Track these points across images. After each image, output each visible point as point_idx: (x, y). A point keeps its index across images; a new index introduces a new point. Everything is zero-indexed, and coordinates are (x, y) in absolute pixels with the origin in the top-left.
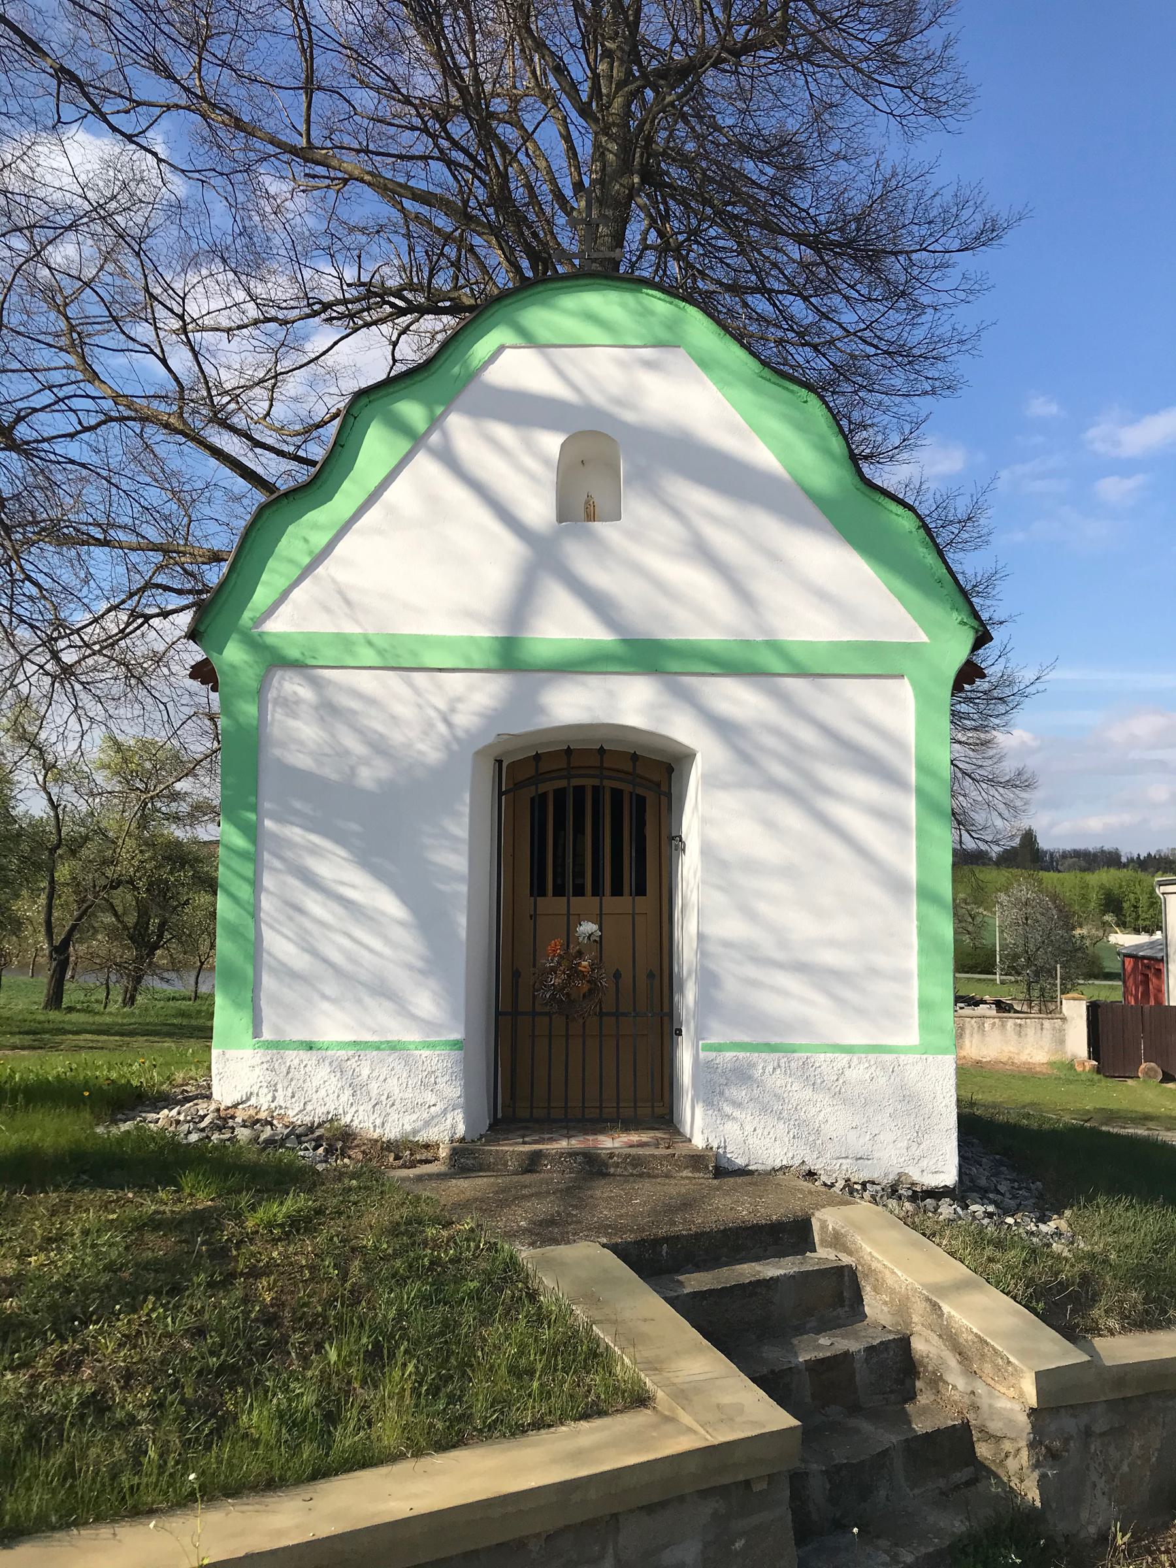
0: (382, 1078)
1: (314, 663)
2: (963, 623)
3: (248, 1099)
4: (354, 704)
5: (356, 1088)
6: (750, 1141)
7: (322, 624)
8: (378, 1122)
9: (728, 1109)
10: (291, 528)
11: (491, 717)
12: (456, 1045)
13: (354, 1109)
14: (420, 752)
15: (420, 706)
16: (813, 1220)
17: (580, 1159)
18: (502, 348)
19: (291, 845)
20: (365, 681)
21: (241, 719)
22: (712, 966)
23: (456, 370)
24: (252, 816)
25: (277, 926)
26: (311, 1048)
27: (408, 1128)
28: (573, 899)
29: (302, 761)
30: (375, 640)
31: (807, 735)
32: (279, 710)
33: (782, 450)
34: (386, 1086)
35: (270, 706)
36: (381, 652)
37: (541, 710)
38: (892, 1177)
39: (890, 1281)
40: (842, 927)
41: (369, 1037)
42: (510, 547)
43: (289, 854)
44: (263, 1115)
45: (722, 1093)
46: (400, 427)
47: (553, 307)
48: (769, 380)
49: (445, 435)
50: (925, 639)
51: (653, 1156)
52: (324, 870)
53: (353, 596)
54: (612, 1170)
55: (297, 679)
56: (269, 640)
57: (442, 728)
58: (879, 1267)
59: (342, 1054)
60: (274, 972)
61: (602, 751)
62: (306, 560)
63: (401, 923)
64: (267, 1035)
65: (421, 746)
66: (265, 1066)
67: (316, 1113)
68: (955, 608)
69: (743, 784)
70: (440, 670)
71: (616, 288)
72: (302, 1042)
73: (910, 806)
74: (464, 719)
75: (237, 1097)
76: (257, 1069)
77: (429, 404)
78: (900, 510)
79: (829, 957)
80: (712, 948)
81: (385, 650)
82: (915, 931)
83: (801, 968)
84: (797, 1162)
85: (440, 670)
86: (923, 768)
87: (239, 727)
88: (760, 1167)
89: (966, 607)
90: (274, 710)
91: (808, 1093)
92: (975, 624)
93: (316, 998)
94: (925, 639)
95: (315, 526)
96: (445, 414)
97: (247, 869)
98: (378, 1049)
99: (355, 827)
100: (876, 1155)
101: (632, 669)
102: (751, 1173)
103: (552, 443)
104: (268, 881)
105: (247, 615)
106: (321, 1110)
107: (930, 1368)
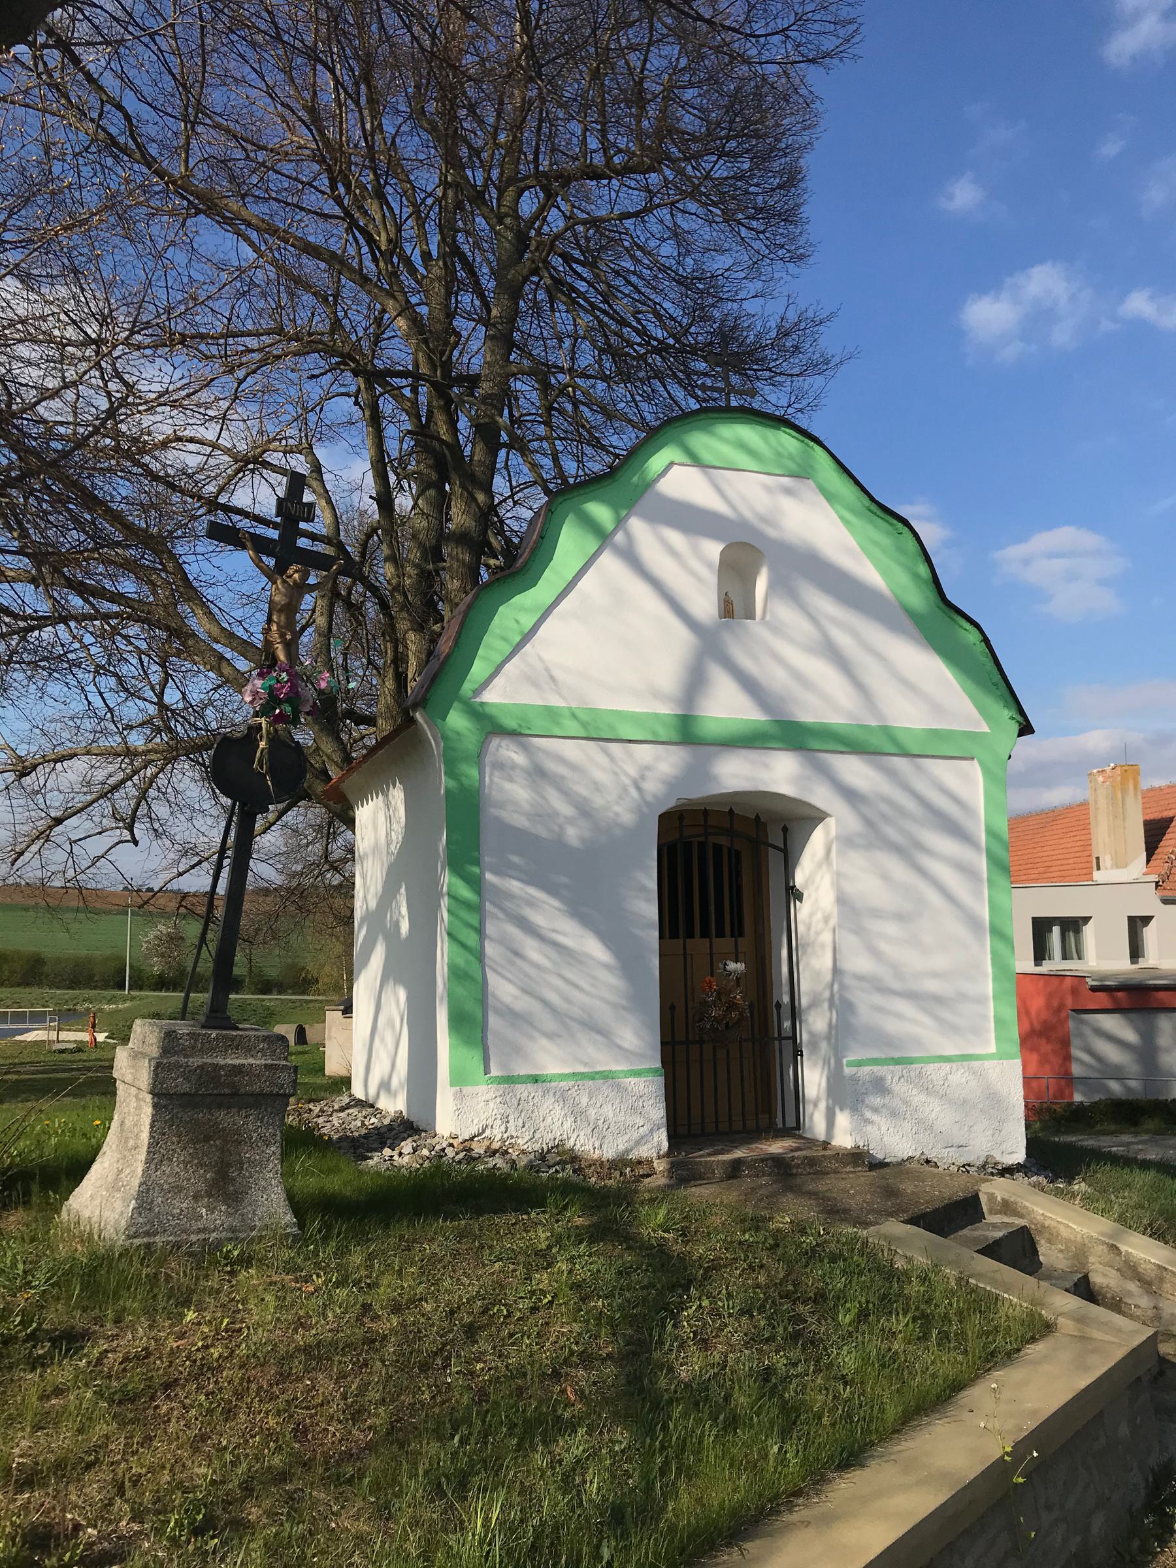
0: (598, 1105)
1: (528, 732)
2: (1012, 718)
3: (484, 1131)
4: (561, 770)
5: (578, 1114)
6: (885, 1139)
7: (530, 697)
8: (597, 1145)
9: (868, 1114)
10: (502, 609)
11: (672, 784)
12: (655, 1071)
13: (575, 1135)
14: (617, 814)
15: (616, 774)
16: (981, 1195)
17: (770, 1163)
18: (672, 464)
19: (509, 896)
20: (571, 750)
21: (465, 781)
22: (849, 996)
23: (635, 479)
24: (476, 870)
25: (500, 969)
26: (536, 1081)
27: (621, 1147)
28: (715, 940)
29: (520, 821)
30: (577, 712)
31: (909, 804)
32: (496, 773)
33: (884, 572)
34: (601, 1111)
35: (488, 770)
36: (584, 725)
37: (713, 779)
38: (982, 1159)
39: (1065, 1233)
40: (940, 962)
41: (581, 1069)
42: (682, 636)
43: (508, 904)
44: (496, 1146)
45: (863, 1101)
46: (591, 525)
47: (713, 434)
48: (875, 514)
49: (629, 536)
50: (986, 729)
51: (824, 1156)
52: (538, 919)
53: (557, 673)
54: (794, 1171)
55: (512, 746)
56: (488, 710)
57: (634, 793)
58: (1053, 1223)
59: (564, 1084)
60: (497, 1011)
61: (706, 812)
62: (518, 639)
63: (606, 966)
64: (495, 1072)
65: (618, 809)
66: (498, 1100)
67: (545, 1140)
68: (1006, 706)
69: (869, 846)
70: (630, 741)
71: (760, 424)
72: (529, 1076)
73: (983, 864)
74: (652, 787)
75: (473, 1130)
76: (491, 1104)
77: (615, 506)
78: (967, 626)
79: (932, 986)
80: (848, 981)
81: (588, 723)
82: (989, 962)
83: (912, 996)
84: (918, 1154)
85: (630, 741)
86: (991, 832)
87: (463, 788)
88: (894, 1160)
89: (1014, 706)
90: (491, 775)
91: (922, 1097)
92: (1021, 719)
93: (536, 1034)
94: (986, 729)
95: (522, 609)
96: (628, 516)
97: (474, 919)
98: (593, 1079)
99: (564, 880)
100: (971, 1143)
101: (781, 746)
102: (887, 1165)
103: (714, 549)
104: (490, 928)
105: (467, 687)
106: (548, 1137)
107: (1109, 1295)
